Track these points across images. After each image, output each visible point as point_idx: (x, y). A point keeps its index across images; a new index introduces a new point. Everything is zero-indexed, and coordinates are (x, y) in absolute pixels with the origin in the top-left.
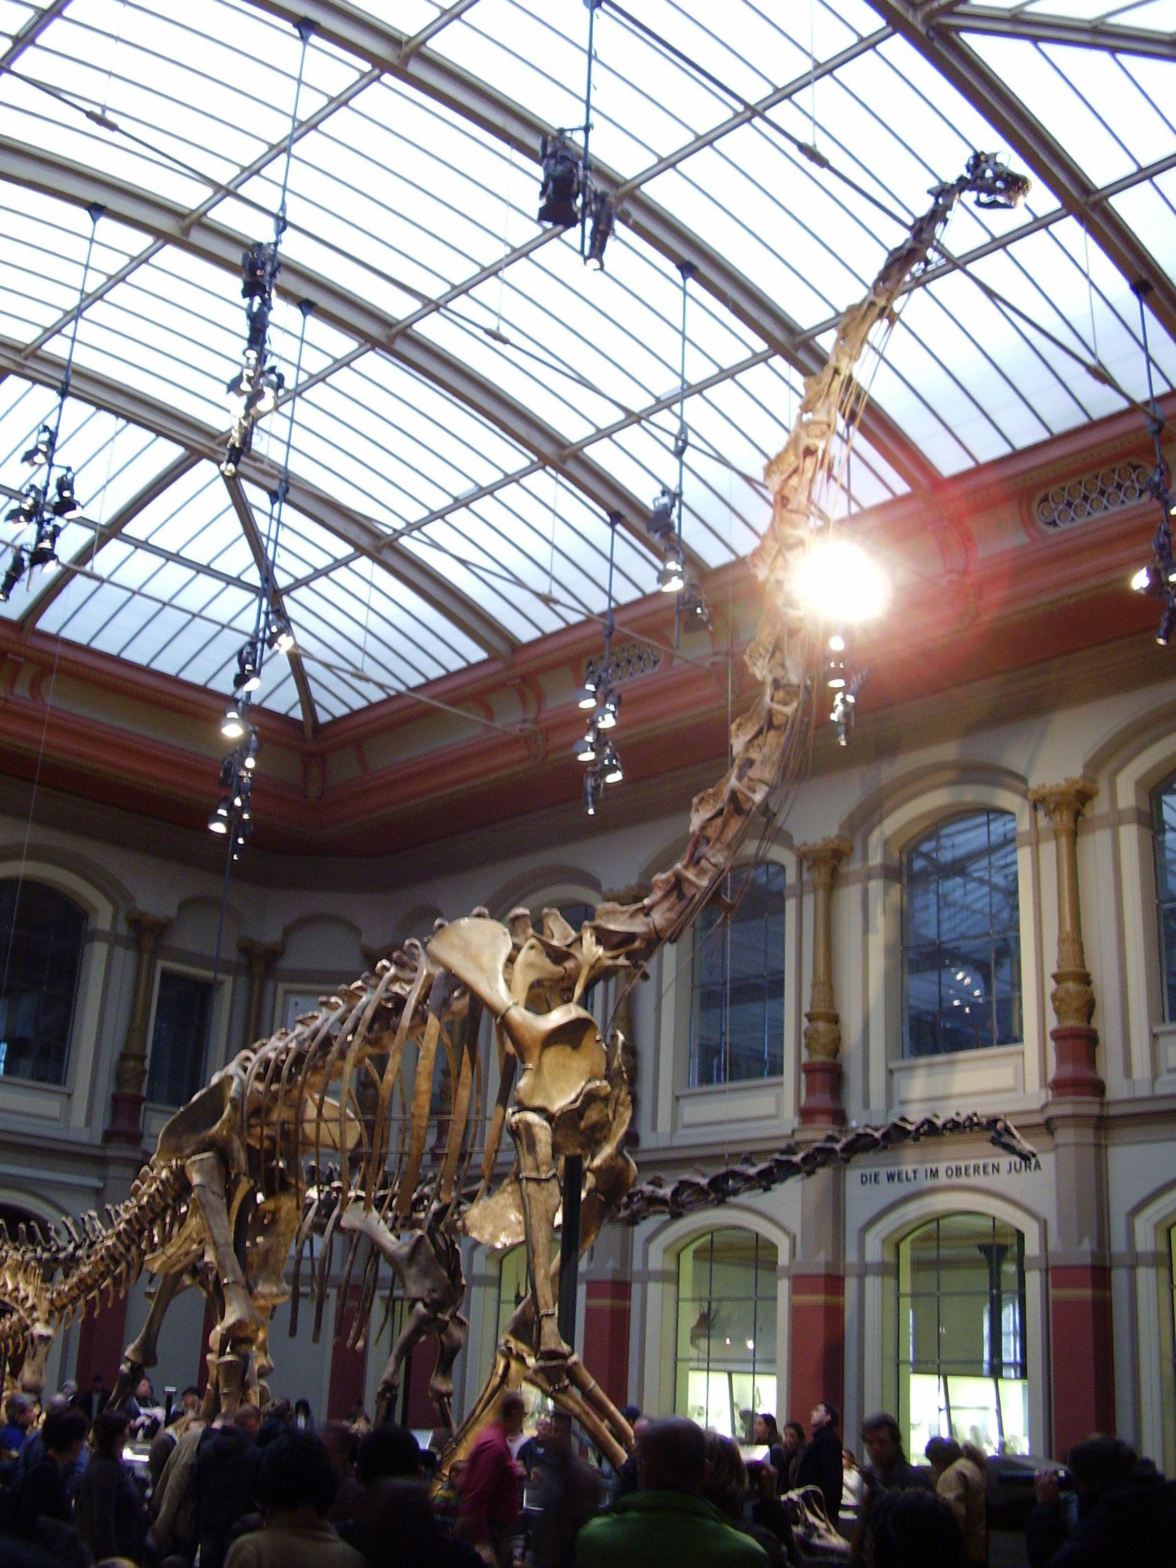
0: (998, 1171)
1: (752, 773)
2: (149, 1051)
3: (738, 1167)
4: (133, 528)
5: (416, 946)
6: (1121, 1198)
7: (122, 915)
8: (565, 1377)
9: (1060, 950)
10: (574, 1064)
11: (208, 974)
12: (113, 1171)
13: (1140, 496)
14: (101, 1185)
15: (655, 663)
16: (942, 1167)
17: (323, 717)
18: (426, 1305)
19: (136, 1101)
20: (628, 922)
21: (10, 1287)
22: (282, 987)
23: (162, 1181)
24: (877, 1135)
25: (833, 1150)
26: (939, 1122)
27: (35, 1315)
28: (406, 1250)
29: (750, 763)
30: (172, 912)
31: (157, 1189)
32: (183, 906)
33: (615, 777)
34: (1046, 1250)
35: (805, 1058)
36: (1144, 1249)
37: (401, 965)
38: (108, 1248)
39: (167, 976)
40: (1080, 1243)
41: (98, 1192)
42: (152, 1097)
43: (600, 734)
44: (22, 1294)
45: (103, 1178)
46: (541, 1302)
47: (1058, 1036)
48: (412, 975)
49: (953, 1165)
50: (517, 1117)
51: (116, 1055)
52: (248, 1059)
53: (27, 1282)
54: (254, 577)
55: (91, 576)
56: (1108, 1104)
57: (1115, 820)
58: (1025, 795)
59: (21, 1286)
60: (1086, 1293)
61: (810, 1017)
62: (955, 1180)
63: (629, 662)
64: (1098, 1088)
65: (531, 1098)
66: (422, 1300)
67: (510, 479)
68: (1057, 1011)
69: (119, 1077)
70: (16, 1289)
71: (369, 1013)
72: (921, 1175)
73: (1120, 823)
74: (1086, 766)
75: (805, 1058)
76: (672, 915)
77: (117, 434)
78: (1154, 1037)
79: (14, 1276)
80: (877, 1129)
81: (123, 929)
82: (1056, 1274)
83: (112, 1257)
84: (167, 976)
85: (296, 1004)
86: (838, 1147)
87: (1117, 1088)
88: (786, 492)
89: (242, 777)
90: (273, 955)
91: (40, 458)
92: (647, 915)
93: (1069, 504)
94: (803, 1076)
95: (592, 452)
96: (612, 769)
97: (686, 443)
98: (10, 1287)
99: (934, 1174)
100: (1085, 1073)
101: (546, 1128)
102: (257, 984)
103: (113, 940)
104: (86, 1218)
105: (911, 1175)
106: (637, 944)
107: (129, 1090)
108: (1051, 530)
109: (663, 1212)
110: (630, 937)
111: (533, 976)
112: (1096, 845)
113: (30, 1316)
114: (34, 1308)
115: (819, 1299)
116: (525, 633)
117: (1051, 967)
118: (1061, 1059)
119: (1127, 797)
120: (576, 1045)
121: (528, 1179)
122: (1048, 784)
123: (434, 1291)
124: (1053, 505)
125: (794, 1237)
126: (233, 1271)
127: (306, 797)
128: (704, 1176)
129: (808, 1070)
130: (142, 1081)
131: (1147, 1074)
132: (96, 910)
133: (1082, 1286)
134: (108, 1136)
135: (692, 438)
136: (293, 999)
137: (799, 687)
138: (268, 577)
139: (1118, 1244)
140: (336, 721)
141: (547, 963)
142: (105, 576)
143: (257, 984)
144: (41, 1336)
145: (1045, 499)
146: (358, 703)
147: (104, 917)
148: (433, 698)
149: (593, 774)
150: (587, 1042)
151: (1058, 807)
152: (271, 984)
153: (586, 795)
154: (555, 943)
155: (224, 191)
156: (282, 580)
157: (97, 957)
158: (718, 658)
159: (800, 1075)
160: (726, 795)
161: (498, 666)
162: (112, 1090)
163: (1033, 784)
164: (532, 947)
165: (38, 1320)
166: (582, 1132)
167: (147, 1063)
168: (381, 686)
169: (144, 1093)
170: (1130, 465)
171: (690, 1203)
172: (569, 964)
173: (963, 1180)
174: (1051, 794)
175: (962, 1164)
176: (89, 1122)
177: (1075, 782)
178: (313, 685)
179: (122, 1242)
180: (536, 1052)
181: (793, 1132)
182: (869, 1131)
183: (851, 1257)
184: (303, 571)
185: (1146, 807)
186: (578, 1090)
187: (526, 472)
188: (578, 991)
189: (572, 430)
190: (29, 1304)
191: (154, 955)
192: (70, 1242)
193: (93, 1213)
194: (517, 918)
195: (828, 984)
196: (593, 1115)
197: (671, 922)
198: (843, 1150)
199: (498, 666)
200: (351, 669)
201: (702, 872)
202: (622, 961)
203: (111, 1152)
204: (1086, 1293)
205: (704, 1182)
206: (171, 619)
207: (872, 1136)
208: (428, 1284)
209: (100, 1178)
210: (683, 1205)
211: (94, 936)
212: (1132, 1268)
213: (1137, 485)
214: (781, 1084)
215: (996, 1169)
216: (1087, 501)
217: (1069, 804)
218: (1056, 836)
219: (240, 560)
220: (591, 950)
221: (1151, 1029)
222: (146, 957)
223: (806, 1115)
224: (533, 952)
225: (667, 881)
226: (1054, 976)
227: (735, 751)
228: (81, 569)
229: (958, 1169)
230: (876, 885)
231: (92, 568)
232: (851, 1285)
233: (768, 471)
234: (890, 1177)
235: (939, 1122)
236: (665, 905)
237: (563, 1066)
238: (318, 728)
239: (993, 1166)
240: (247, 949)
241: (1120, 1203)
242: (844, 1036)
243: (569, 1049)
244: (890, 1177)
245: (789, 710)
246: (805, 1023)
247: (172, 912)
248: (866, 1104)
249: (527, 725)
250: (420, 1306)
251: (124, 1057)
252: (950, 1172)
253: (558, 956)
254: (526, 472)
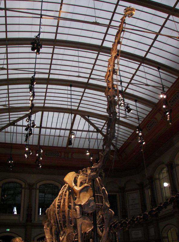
10: (87, 195)
11: (115, 194)
17: (119, 149)
24: (175, 197)
33: (144, 143)
43: (140, 136)
54: (95, 130)
63: (152, 124)
85: (129, 195)
86: (168, 201)
88: (108, 79)
96: (143, 142)
106: (98, 169)
110: (96, 168)
111: (81, 180)
120: (87, 191)
135: (164, 87)
140: (120, 148)
146: (122, 145)
150: (89, 190)
155: (89, 78)
156: (100, 129)
166: (90, 208)
168: (123, 141)
180: (78, 194)
182: (173, 196)
184: (102, 127)
194: (84, 170)
206: (56, 138)
207: (174, 197)
219: (92, 128)
224: (82, 176)
233: (105, 78)
237: (85, 195)
243: (86, 192)
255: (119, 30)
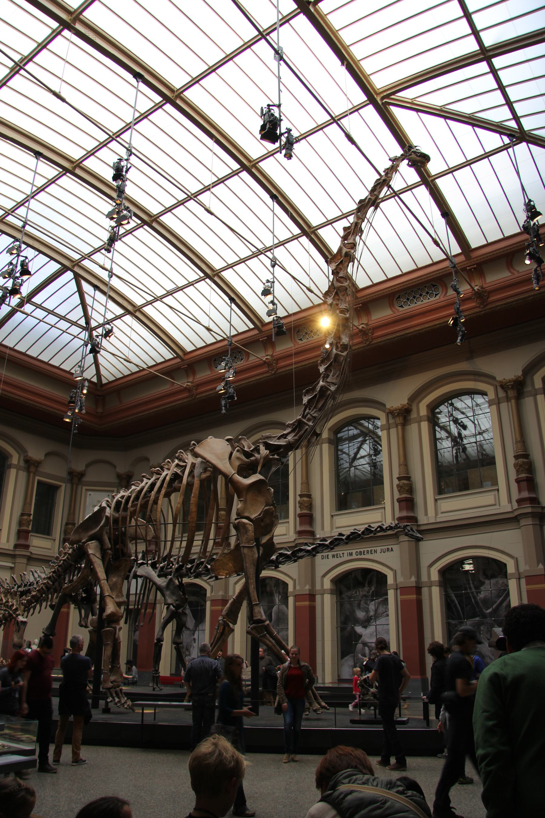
0: (376, 552)
1: (329, 380)
2: (32, 512)
3: (303, 547)
4: (37, 299)
5: (182, 453)
6: (425, 561)
7: (22, 458)
8: (264, 631)
9: (400, 469)
12: (18, 560)
13: (435, 297)
14: (13, 566)
15: (242, 359)
16: (354, 552)
17: (104, 381)
18: (174, 606)
19: (28, 532)
20: (278, 441)
21: (4, 601)
22: (84, 488)
23: (69, 554)
24: (360, 533)
25: (342, 539)
26: (384, 527)
27: (18, 613)
28: (165, 584)
29: (328, 376)
30: (42, 457)
31: (67, 558)
32: (47, 455)
34: (396, 582)
35: (298, 511)
36: (434, 580)
37: (180, 460)
38: (44, 584)
39: (39, 482)
40: (411, 578)
41: (11, 568)
42: (32, 531)
44: (10, 604)
45: (14, 563)
46: (253, 599)
47: (399, 500)
48: (184, 464)
49: (358, 550)
50: (238, 521)
51: (19, 514)
52: (107, 501)
53: (12, 598)
54: (82, 322)
55: (23, 313)
56: (420, 525)
57: (419, 421)
58: (384, 411)
59: (10, 600)
60: (414, 597)
61: (301, 496)
62: (359, 557)
64: (414, 519)
65: (243, 513)
66: (172, 604)
67: (191, 284)
68: (399, 491)
69: (20, 523)
70: (7, 602)
71: (168, 478)
72: (346, 555)
73: (421, 421)
74: (409, 399)
75: (298, 511)
76: (296, 438)
77: (35, 257)
78: (436, 500)
79: (6, 596)
80: (360, 531)
81: (22, 464)
82: (403, 590)
83: (47, 587)
84: (39, 482)
85: (90, 495)
86: (344, 538)
87: (422, 520)
89: (82, 397)
90: (82, 475)
91: (15, 252)
92: (285, 438)
93: (408, 299)
94: (298, 519)
95: (224, 274)
97: (276, 264)
98: (4, 601)
99: (351, 554)
100: (411, 514)
101: (251, 525)
102: (75, 486)
103: (18, 468)
104: (22, 575)
105: (342, 555)
107: (24, 528)
108: (401, 309)
109: (272, 566)
111: (237, 463)
112: (413, 428)
113: (15, 613)
114: (17, 609)
115: (307, 603)
116: (189, 348)
117: (396, 475)
118: (401, 509)
119: (423, 411)
121: (244, 547)
122: (394, 407)
123: (177, 601)
124: (402, 299)
125: (295, 580)
126: (108, 591)
127: (97, 412)
128: (288, 551)
129: (300, 516)
130: (29, 524)
131: (434, 514)
132: (11, 456)
133: (413, 594)
134: (16, 546)
136: (89, 493)
137: (347, 345)
138: (88, 322)
139: (424, 578)
140: (110, 383)
141: (244, 458)
142: (29, 313)
143: (75, 486)
144: (22, 622)
145: (399, 297)
147: (15, 459)
148: (154, 371)
149: (225, 398)
151: (398, 415)
152: (80, 487)
153: (222, 406)
154: (245, 449)
157: (12, 473)
158: (268, 357)
159: (296, 518)
160: (318, 388)
161: (178, 360)
162: (17, 528)
163: (388, 406)
164: (238, 451)
165: (19, 615)
167: (32, 517)
169: (30, 528)
170: (432, 285)
171: (283, 562)
172: (252, 458)
173: (363, 556)
174: (396, 410)
175: (362, 550)
176: (8, 541)
177: (405, 405)
178: (101, 368)
179: (51, 581)
181: (295, 540)
183: (318, 587)
185: (430, 415)
186: (261, 510)
187: (197, 281)
188: (259, 468)
189: (217, 264)
190: (15, 607)
191: (35, 474)
192: (15, 585)
193: (25, 573)
195: (307, 482)
196: (267, 521)
197: (297, 441)
198: (346, 539)
199: (178, 360)
200: (124, 357)
201: (309, 420)
202: (276, 457)
203: (17, 553)
204: (414, 597)
205: (289, 553)
207: (357, 533)
208: (174, 598)
209: (13, 563)
210: (280, 563)
211: (10, 466)
212: (430, 587)
213: (434, 293)
214: (288, 522)
215: (376, 551)
216: (415, 298)
217: (403, 414)
218: (397, 427)
219: (77, 315)
220: (264, 451)
221: (434, 498)
222: (32, 475)
223: (300, 533)
224: (238, 453)
225: (293, 424)
226: (398, 478)
227: (321, 372)
228: (20, 309)
229: (361, 552)
230: (326, 447)
231: (24, 309)
232: (318, 597)
234: (333, 556)
235: (384, 527)
236: (293, 434)
238: (103, 385)
239: (374, 550)
240: (71, 473)
241: (425, 563)
242: (313, 503)
244: (333, 556)
245: (344, 354)
246: (298, 498)
247: (42, 457)
248: (323, 529)
249: (189, 384)
250: (172, 607)
251: (22, 515)
252: (357, 554)
253: (248, 455)
254: (197, 281)
255: (384, 181)
